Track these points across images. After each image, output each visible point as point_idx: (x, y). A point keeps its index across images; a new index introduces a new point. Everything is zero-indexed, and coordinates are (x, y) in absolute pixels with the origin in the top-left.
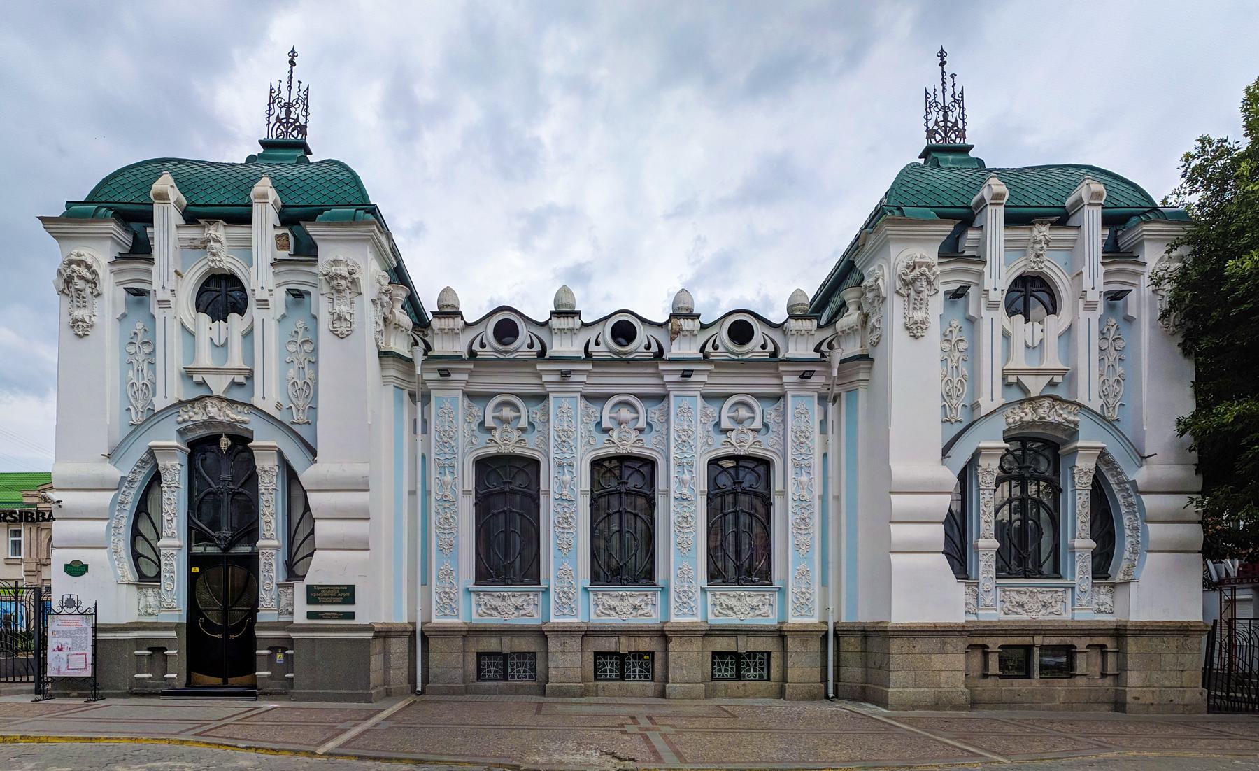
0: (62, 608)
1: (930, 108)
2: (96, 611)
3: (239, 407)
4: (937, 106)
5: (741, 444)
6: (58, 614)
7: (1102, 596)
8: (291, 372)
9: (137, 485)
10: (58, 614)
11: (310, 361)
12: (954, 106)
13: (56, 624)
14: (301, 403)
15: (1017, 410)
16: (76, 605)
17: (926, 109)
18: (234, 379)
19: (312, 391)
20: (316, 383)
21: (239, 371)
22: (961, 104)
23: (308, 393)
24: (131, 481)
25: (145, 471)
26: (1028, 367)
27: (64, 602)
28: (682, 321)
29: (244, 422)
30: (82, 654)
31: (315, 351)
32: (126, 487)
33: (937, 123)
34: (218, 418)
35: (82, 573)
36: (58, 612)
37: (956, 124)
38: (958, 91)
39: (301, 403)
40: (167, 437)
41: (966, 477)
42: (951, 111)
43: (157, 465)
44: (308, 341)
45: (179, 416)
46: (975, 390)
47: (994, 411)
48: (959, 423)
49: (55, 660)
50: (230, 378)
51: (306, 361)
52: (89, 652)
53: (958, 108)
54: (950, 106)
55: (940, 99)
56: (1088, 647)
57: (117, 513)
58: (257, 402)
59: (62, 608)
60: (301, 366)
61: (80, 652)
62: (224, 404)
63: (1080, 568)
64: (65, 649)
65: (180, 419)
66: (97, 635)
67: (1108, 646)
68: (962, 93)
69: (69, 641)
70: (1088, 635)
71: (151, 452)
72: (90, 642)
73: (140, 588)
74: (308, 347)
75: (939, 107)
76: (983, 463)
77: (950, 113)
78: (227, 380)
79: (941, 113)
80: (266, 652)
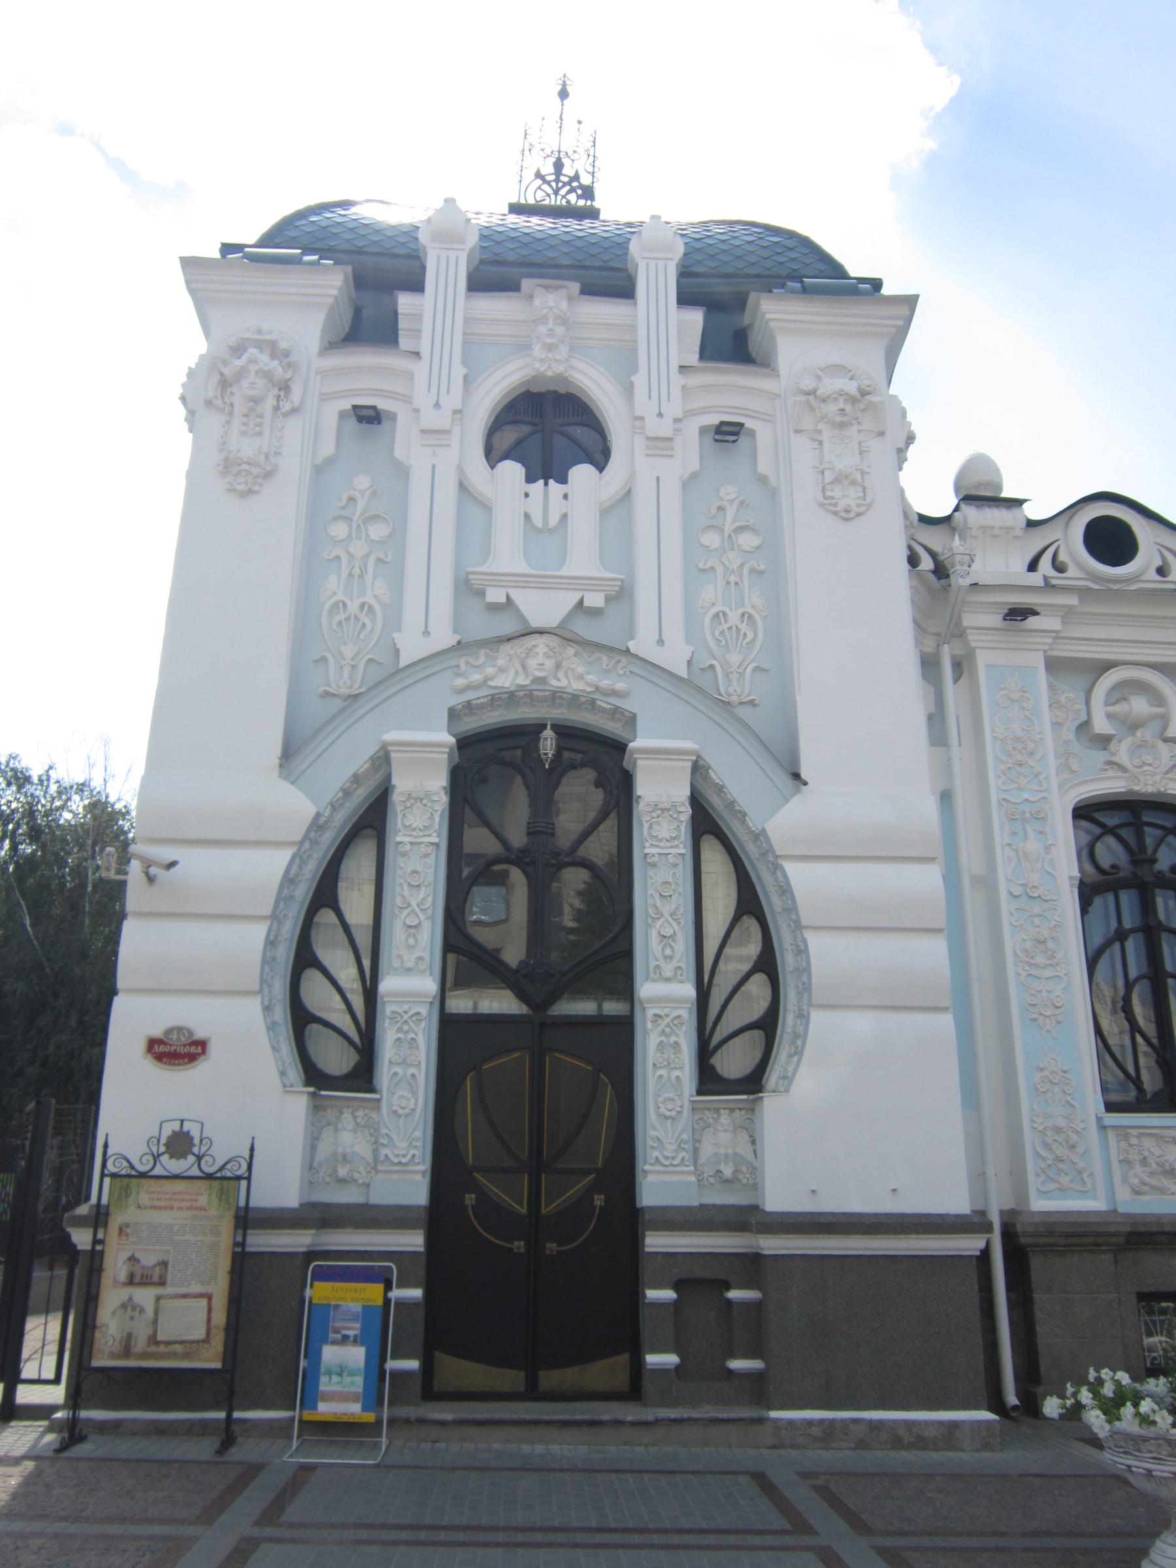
0: (156, 1158)
3: (605, 659)
8: (710, 593)
10: (143, 1175)
11: (752, 570)
16: (195, 1150)
18: (581, 602)
23: (750, 636)
27: (163, 1140)
29: (613, 693)
30: (201, 1295)
35: (192, 1058)
36: (142, 1168)
39: (734, 658)
45: (458, 675)
49: (119, 1312)
52: (220, 1288)
59: (156, 1158)
60: (732, 579)
62: (570, 651)
65: (460, 682)
66: (250, 1240)
71: (383, 759)
72: (225, 1262)
74: (747, 541)
78: (564, 602)
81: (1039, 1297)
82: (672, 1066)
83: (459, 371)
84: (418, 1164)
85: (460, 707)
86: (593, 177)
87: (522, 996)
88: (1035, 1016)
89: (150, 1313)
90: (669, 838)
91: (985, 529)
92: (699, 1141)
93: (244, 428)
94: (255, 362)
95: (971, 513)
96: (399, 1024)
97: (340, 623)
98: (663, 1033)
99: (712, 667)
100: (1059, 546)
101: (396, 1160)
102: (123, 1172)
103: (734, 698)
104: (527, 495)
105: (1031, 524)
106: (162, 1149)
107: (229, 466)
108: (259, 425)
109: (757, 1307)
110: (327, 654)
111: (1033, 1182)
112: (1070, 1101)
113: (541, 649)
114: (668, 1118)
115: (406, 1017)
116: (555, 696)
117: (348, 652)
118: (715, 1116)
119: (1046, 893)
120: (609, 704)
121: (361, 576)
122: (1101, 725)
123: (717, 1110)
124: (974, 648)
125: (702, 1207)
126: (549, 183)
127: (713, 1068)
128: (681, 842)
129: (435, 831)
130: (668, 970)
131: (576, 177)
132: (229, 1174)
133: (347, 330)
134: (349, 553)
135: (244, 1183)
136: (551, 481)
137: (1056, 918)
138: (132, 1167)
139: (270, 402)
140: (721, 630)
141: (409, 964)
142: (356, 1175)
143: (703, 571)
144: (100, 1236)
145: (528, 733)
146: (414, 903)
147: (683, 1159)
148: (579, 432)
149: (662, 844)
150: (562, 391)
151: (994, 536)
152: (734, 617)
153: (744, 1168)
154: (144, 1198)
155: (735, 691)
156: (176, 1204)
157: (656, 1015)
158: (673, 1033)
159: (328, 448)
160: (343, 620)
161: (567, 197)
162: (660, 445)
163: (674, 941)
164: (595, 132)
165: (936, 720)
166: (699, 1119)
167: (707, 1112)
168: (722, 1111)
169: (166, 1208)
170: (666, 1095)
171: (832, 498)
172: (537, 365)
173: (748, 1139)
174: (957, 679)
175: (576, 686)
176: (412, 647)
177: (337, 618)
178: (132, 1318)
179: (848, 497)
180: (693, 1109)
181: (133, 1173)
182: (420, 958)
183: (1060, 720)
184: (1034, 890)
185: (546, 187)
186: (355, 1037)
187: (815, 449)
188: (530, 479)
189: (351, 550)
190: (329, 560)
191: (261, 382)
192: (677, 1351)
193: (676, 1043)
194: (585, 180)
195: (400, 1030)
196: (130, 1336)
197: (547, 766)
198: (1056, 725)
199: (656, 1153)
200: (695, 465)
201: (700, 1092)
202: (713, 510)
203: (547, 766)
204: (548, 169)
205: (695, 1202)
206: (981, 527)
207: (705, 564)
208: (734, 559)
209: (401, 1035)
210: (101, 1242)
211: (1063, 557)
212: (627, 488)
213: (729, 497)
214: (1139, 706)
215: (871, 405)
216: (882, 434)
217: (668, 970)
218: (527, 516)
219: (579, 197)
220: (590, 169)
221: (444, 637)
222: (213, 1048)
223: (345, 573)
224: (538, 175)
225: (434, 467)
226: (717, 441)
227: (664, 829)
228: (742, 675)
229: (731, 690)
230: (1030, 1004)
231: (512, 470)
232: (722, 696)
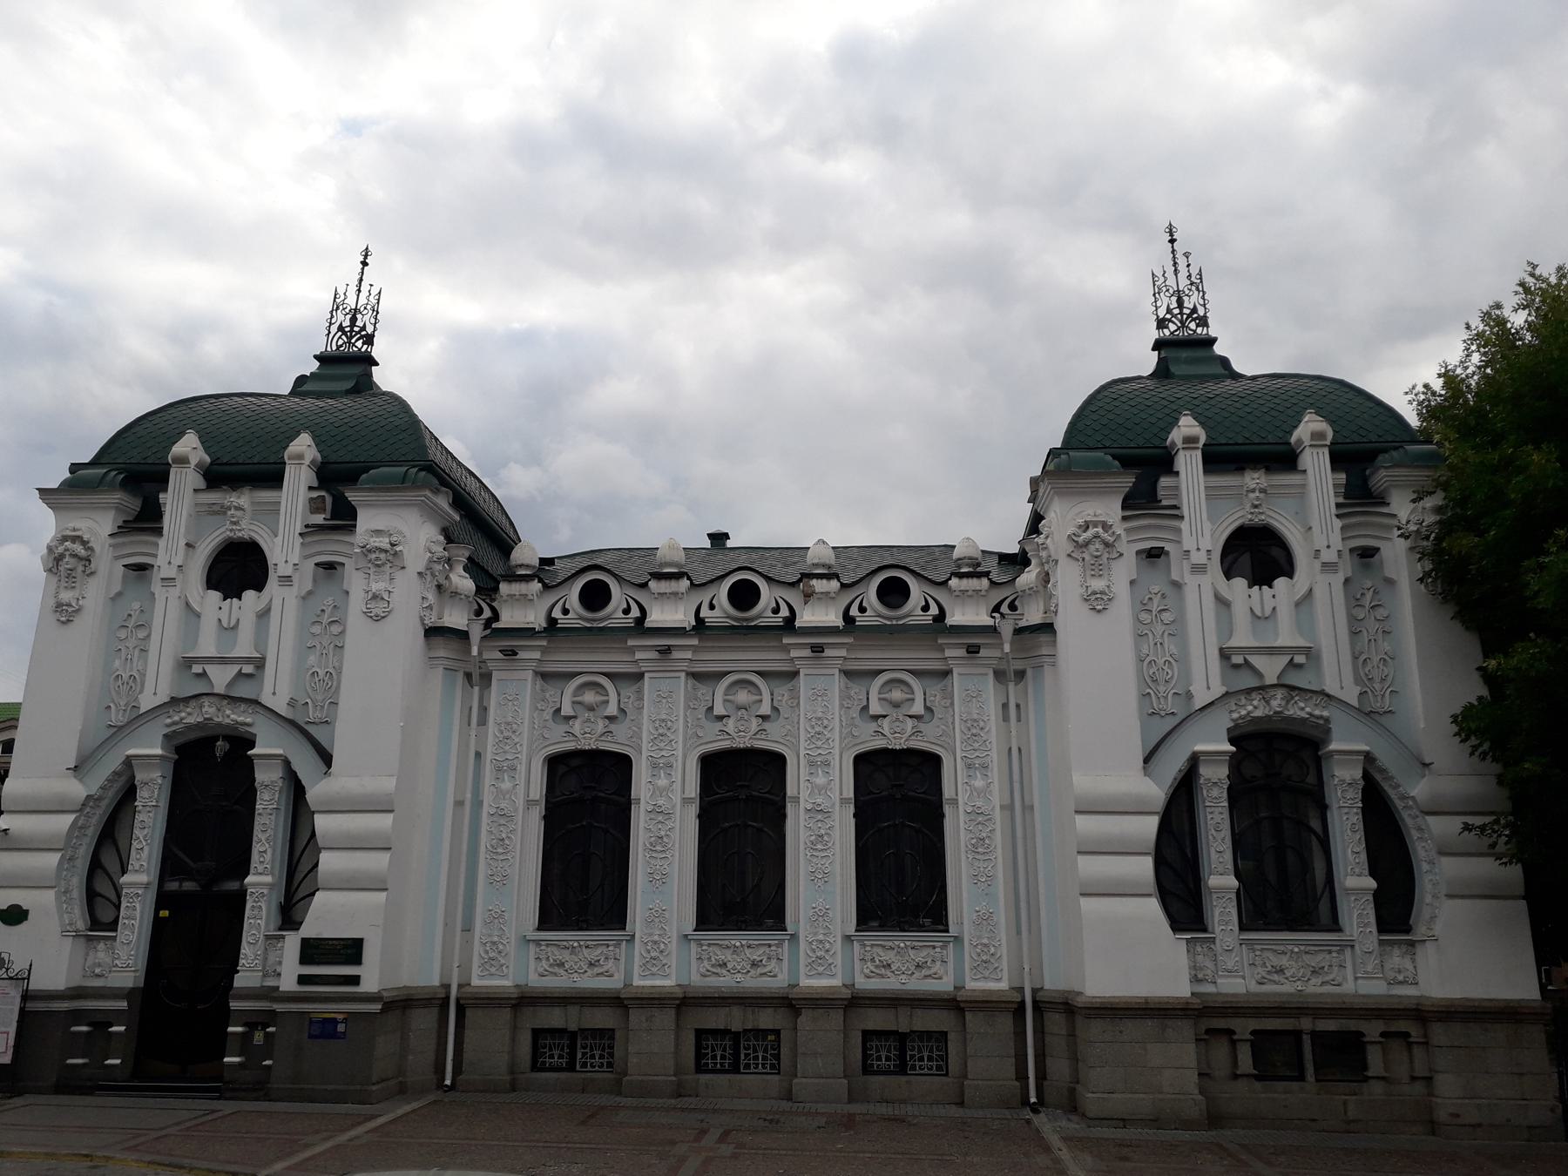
1: (1159, 293)
4: (1168, 290)
5: (896, 735)
7: (1397, 960)
8: (312, 659)
9: (104, 803)
12: (1190, 290)
14: (320, 697)
15: (1244, 701)
17: (1154, 295)
18: (241, 669)
19: (335, 683)
20: (340, 673)
21: (248, 660)
22: (1200, 287)
23: (330, 684)
24: (100, 799)
25: (117, 786)
26: (1257, 645)
28: (814, 582)
29: (248, 725)
30: (5, 1033)
31: (343, 632)
32: (91, 807)
33: (1169, 311)
34: (216, 719)
37: (1194, 310)
38: (1194, 272)
39: (320, 697)
40: (150, 746)
41: (1185, 790)
42: (1187, 295)
43: (134, 777)
44: (337, 621)
45: (169, 717)
46: (1187, 675)
47: (1212, 703)
48: (1171, 716)
50: (235, 668)
51: (332, 645)
52: (12, 1030)
53: (1196, 293)
54: (1186, 290)
55: (1171, 282)
56: (1383, 1034)
57: (74, 841)
58: (266, 699)
60: (324, 652)
63: (1357, 916)
65: (169, 721)
67: (1413, 1034)
68: (1200, 274)
70: (1378, 1017)
71: (128, 762)
73: (89, 939)
74: (335, 629)
75: (1171, 291)
76: (1206, 772)
77: (1186, 298)
79: (1174, 299)
80: (239, 1029)
81: (468, 1033)
83: (182, 543)
86: (375, 327)
91: (511, 596)
93: (66, 585)
94: (68, 550)
98: (255, 901)
107: (59, 606)
110: (112, 705)
111: (476, 970)
113: (206, 704)
116: (219, 725)
122: (567, 710)
125: (263, 987)
130: (260, 869)
131: (364, 328)
135: (26, 981)
139: (80, 568)
141: (137, 868)
146: (141, 838)
149: (265, 803)
151: (517, 600)
158: (259, 901)
162: (286, 580)
164: (380, 293)
170: (253, 932)
171: (369, 609)
172: (228, 533)
175: (227, 721)
176: (147, 702)
179: (378, 608)
183: (543, 708)
185: (343, 337)
191: (73, 561)
194: (370, 329)
195: (128, 902)
199: (244, 961)
200: (309, 586)
202: (319, 612)
205: (259, 985)
206: (508, 596)
209: (129, 904)
214: (590, 697)
215: (396, 554)
216: (403, 568)
217: (260, 869)
219: (363, 344)
220: (373, 321)
221: (163, 697)
223: (123, 658)
224: (341, 328)
231: (215, 595)
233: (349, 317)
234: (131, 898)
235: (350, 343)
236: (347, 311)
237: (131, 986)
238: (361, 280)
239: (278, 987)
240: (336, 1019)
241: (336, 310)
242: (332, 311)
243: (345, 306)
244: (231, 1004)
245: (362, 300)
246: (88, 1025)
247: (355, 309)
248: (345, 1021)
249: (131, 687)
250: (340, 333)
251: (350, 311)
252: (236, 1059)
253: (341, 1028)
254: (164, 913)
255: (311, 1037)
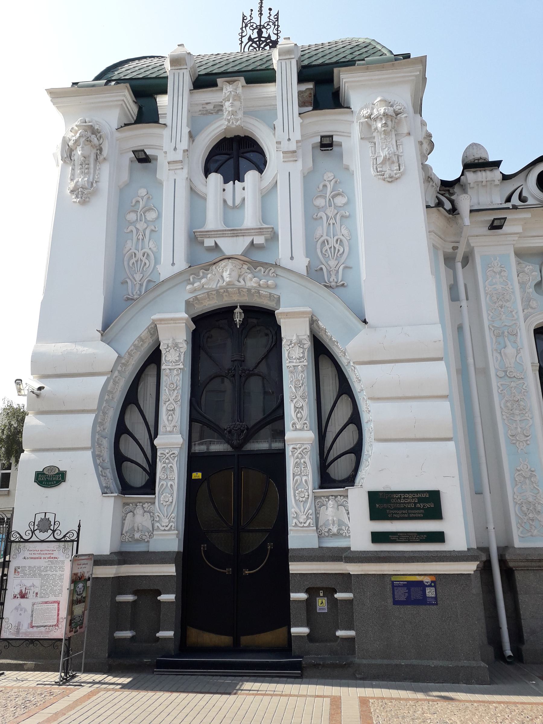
0: (33, 532)
2: (78, 536)
6: (26, 541)
10: (26, 541)
11: (342, 217)
13: (21, 556)
16: (52, 528)
18: (252, 242)
21: (260, 231)
27: (36, 523)
36: (26, 538)
39: (332, 263)
59: (33, 532)
60: (331, 222)
61: (53, 599)
64: (31, 595)
69: (37, 582)
82: (303, 474)
84: (174, 530)
85: (191, 300)
86: (278, 36)
87: (228, 442)
88: (514, 442)
89: (30, 612)
90: (299, 358)
91: (477, 183)
92: (319, 514)
95: (471, 176)
96: (164, 460)
97: (133, 263)
99: (321, 269)
100: (523, 188)
101: (163, 528)
102: (17, 540)
103: (333, 284)
104: (224, 190)
105: (505, 178)
106: (36, 527)
108: (88, 168)
109: (349, 602)
112: (536, 487)
114: (302, 502)
115: (167, 455)
117: (138, 277)
118: (327, 500)
119: (518, 375)
120: (266, 292)
121: (143, 239)
123: (328, 497)
124: (473, 247)
126: (255, 43)
127: (328, 475)
128: (306, 359)
129: (182, 362)
132: (68, 539)
133: (135, 119)
134: (137, 230)
136: (236, 181)
137: (524, 387)
138: (21, 537)
140: (326, 249)
142: (144, 537)
143: (316, 219)
144: (5, 572)
145: (229, 311)
147: (310, 523)
148: (251, 155)
150: (242, 135)
152: (332, 242)
153: (343, 528)
154: (27, 554)
155: (334, 280)
156: (43, 556)
157: (294, 448)
158: (302, 458)
159: (125, 176)
160: (135, 262)
161: (265, 48)
163: (303, 410)
165: (453, 289)
166: (318, 502)
167: (323, 498)
168: (330, 497)
169: (37, 558)
173: (345, 511)
174: (464, 266)
177: (133, 260)
178: (20, 614)
180: (315, 497)
181: (22, 540)
182: (175, 426)
184: (511, 373)
185: (254, 45)
186: (147, 468)
187: (372, 147)
188: (226, 182)
189: (138, 226)
190: (128, 233)
192: (308, 625)
193: (304, 462)
194: (274, 38)
195: (164, 463)
196: (19, 623)
197: (238, 327)
198: (522, 285)
201: (321, 487)
203: (238, 327)
204: (255, 35)
205: (316, 546)
207: (317, 216)
208: (331, 212)
210: (6, 575)
211: (524, 194)
212: (275, 181)
213: (329, 179)
218: (225, 201)
220: (276, 32)
222: (68, 477)
224: (250, 39)
225: (175, 180)
226: (322, 150)
227: (297, 353)
228: (337, 272)
229: (331, 280)
230: (511, 435)
231: (215, 178)
232: (327, 283)
233: (256, 30)
234: (167, 459)
235: (259, 47)
236: (254, 26)
237: (177, 551)
238: (261, 7)
239: (349, 548)
240: (422, 582)
241: (245, 27)
242: (242, 28)
243: (252, 24)
244: (290, 567)
245: (265, 19)
246: (135, 593)
247: (260, 25)
248: (433, 584)
249: (145, 263)
250: (251, 43)
251: (257, 26)
252: (305, 630)
253: (430, 592)
254: (197, 475)
255: (396, 602)
